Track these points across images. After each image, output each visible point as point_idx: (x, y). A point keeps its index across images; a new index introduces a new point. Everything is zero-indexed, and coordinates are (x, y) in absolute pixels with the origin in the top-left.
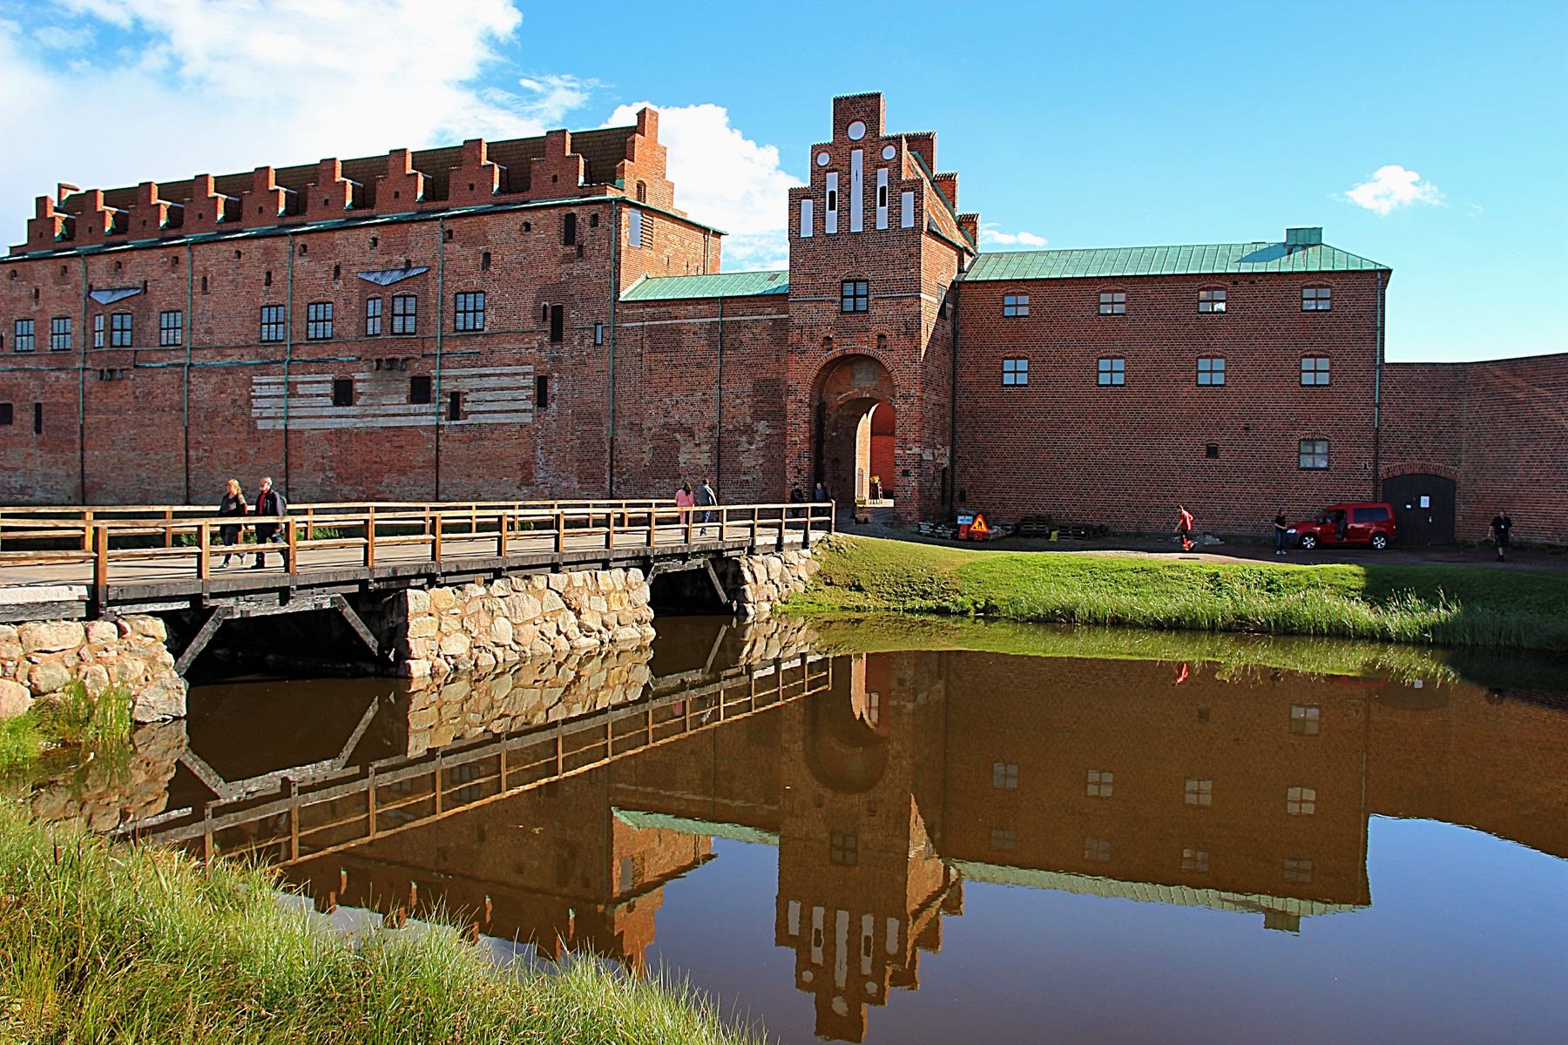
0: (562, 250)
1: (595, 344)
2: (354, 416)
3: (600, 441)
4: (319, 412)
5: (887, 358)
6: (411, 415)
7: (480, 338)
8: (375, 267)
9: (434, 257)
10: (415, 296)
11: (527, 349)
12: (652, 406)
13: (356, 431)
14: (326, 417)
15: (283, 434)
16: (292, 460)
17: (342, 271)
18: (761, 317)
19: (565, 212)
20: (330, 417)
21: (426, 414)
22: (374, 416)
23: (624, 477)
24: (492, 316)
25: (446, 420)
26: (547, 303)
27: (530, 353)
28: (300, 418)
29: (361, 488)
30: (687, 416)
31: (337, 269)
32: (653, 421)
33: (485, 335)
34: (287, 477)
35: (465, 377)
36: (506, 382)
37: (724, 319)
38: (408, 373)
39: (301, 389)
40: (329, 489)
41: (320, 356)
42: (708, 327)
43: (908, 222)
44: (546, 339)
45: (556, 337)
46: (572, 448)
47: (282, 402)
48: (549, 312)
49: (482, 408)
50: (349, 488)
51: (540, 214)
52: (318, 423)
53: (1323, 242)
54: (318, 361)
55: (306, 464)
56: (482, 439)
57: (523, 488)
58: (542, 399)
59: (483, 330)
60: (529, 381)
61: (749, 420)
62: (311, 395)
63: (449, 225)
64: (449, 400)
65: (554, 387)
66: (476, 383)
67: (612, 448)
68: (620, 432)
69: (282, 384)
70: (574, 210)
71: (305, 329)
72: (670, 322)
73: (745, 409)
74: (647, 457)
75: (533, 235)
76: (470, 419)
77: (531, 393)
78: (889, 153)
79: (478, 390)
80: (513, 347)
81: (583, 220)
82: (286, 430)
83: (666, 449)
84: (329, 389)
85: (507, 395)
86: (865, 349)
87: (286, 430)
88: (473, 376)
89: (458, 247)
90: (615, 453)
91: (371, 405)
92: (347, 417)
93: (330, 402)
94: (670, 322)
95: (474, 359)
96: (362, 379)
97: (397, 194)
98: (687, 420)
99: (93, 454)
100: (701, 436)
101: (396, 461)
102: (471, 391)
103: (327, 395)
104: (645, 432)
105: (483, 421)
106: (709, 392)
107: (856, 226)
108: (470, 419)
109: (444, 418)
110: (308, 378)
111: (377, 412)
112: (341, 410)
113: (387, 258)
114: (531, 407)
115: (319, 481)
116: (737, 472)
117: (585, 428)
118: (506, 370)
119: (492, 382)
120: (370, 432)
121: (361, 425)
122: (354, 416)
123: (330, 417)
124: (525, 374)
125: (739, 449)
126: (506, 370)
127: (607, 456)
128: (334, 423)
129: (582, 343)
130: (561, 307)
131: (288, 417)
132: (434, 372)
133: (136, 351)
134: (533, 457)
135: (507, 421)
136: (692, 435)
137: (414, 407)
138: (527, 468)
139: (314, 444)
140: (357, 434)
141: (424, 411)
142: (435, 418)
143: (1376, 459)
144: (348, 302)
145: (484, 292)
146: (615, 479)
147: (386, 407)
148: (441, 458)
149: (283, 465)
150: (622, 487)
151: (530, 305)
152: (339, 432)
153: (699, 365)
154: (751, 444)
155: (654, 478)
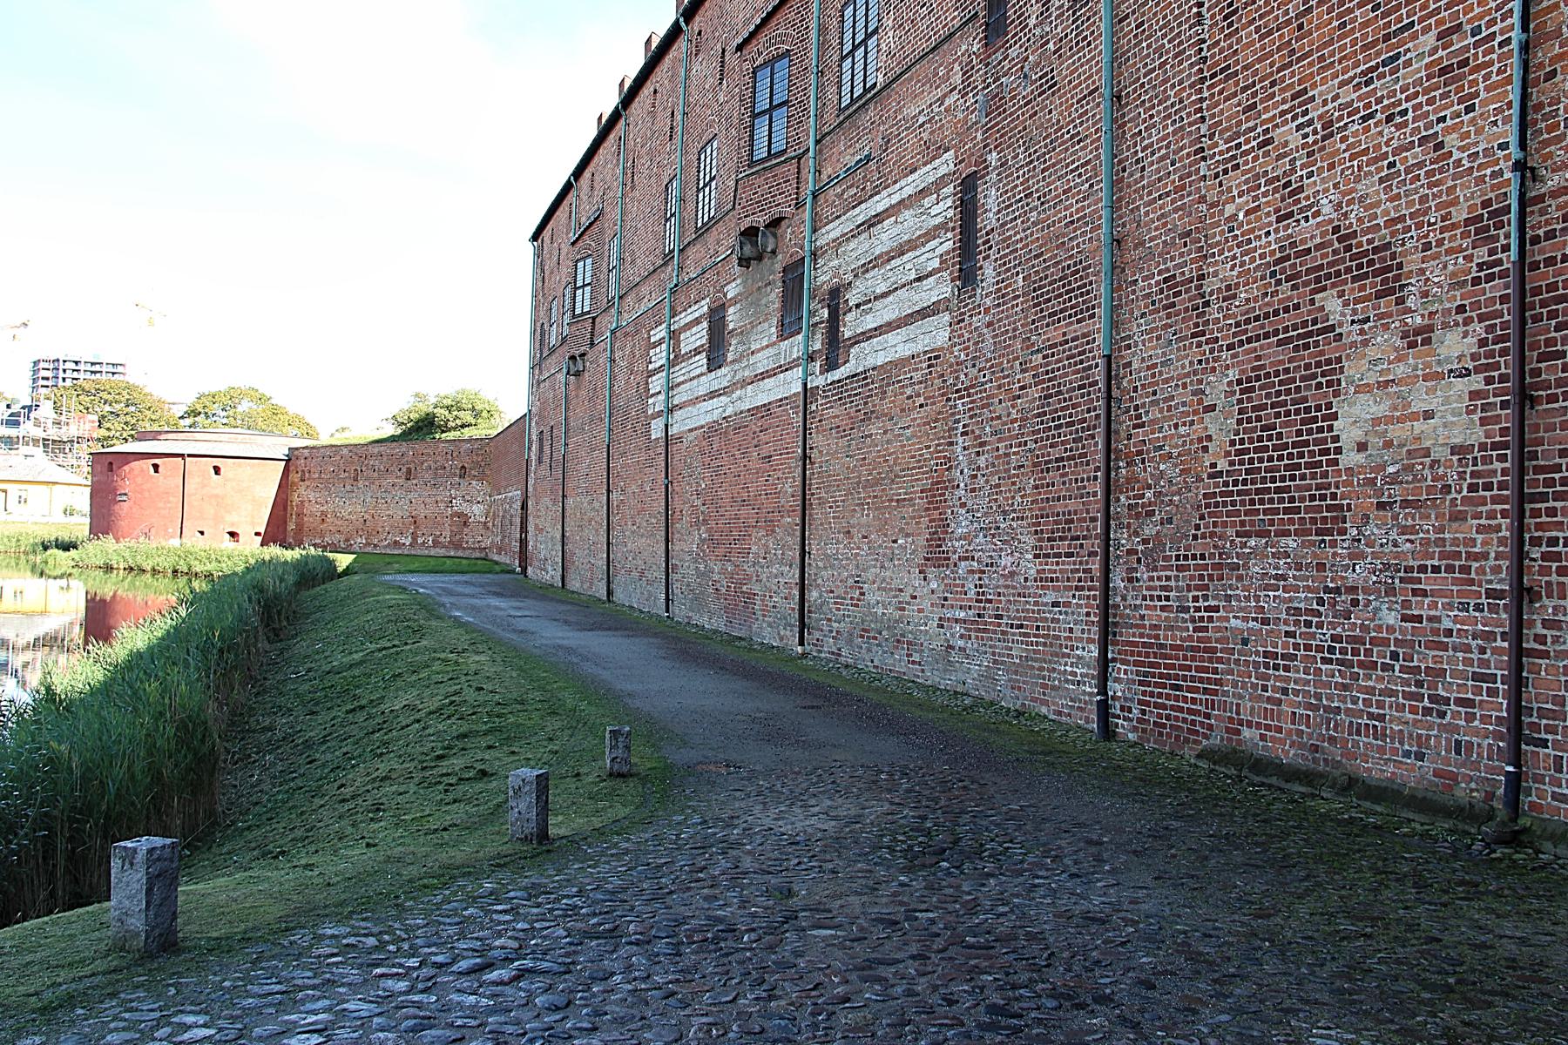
12: (1235, 181)
22: (744, 383)
23: (1149, 531)
30: (1370, 186)
49: (870, 322)
56: (867, 418)
57: (932, 572)
68: (1136, 328)
85: (906, 267)
90: (1125, 424)
99: (570, 501)
104: (1213, 313)
117: (1054, 334)
131: (671, 411)
133: (594, 318)
146: (1122, 537)
148: (814, 482)
150: (1143, 573)
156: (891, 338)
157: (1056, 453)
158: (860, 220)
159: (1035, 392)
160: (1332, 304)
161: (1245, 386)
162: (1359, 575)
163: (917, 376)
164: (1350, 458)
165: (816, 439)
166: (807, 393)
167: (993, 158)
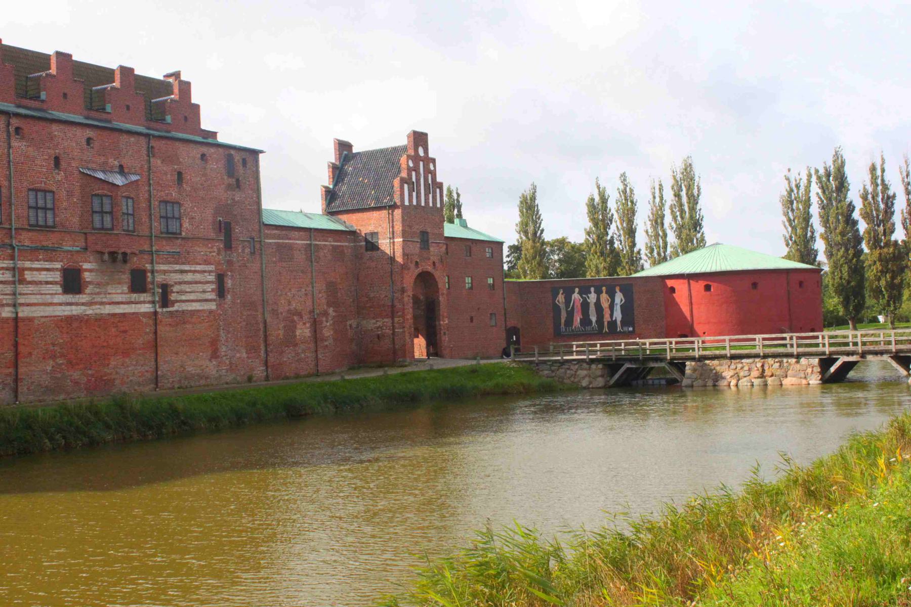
0: (227, 180)
1: (251, 253)
2: (83, 304)
3: (257, 323)
4: (48, 299)
5: (437, 274)
6: (132, 303)
7: (179, 241)
8: (94, 166)
9: (142, 167)
10: (132, 198)
11: (211, 252)
13: (86, 317)
14: (56, 304)
15: (12, 324)
16: (21, 349)
17: (63, 164)
18: (326, 243)
19: (227, 152)
20: (60, 304)
21: (144, 302)
22: (102, 303)
24: (186, 224)
25: (160, 307)
26: (221, 219)
27: (213, 256)
28: (28, 305)
29: (90, 372)
30: (299, 305)
31: (57, 161)
32: (283, 308)
33: (183, 239)
34: (16, 367)
35: (171, 272)
36: (198, 277)
37: (308, 242)
38: (128, 266)
39: (28, 276)
40: (59, 375)
41: (45, 244)
42: (305, 247)
43: (439, 205)
44: (222, 246)
45: (228, 246)
46: (241, 327)
47: (8, 289)
48: (223, 225)
49: (184, 298)
50: (79, 373)
51: (212, 150)
52: (49, 311)
53: (468, 226)
54: (45, 249)
55: (35, 353)
56: (184, 323)
57: (213, 360)
58: (221, 291)
59: (180, 234)
60: (212, 278)
61: (325, 307)
62: (40, 283)
63: (153, 143)
64: (160, 291)
65: (229, 283)
66: (177, 277)
67: (265, 327)
69: (7, 269)
70: (233, 152)
71: (25, 214)
72: (287, 241)
73: (324, 301)
74: (281, 332)
75: (212, 165)
76: (176, 307)
77: (214, 286)
78: (432, 167)
79: (180, 283)
80: (201, 250)
81: (238, 161)
82: (16, 319)
83: (291, 328)
84: (57, 276)
85: (200, 287)
86: (430, 269)
87: (16, 319)
88: (176, 272)
89: (159, 162)
91: (99, 293)
92: (77, 304)
93: (59, 289)
94: (287, 241)
95: (177, 258)
96: (89, 267)
97: (65, 95)
98: (299, 308)
100: (306, 317)
101: (121, 344)
102: (176, 283)
103: (55, 283)
104: (280, 315)
105: (185, 308)
106: (308, 289)
107: (423, 204)
108: (176, 307)
109: (157, 306)
110: (36, 265)
111: (104, 300)
112: (69, 298)
113: (103, 159)
114: (215, 297)
115: (49, 368)
116: (323, 340)
117: (249, 313)
118: (199, 268)
119: (189, 277)
120: (100, 320)
121: (89, 312)
122: (83, 304)
123: (60, 304)
124: (210, 272)
125: (323, 325)
126: (199, 268)
127: (261, 333)
128: (64, 311)
129: (243, 251)
130: (230, 223)
132: (148, 267)
134: (218, 336)
135: (201, 308)
136: (302, 317)
137: (134, 296)
138: (214, 344)
139: (44, 332)
140: (87, 321)
141: (142, 299)
142: (151, 306)
143: (505, 320)
144: (70, 194)
145: (178, 203)
147: (111, 296)
149: (10, 355)
151: (210, 219)
152: (70, 319)
153: (303, 272)
154: (327, 322)
155: (285, 347)
156: (194, 304)
157: (251, 335)
158: (177, 268)
159: (245, 323)
160: (295, 318)
161: (285, 327)
162: (300, 351)
163: (205, 315)
164: (298, 337)
165: (160, 328)
166: (155, 313)
167: (229, 273)
